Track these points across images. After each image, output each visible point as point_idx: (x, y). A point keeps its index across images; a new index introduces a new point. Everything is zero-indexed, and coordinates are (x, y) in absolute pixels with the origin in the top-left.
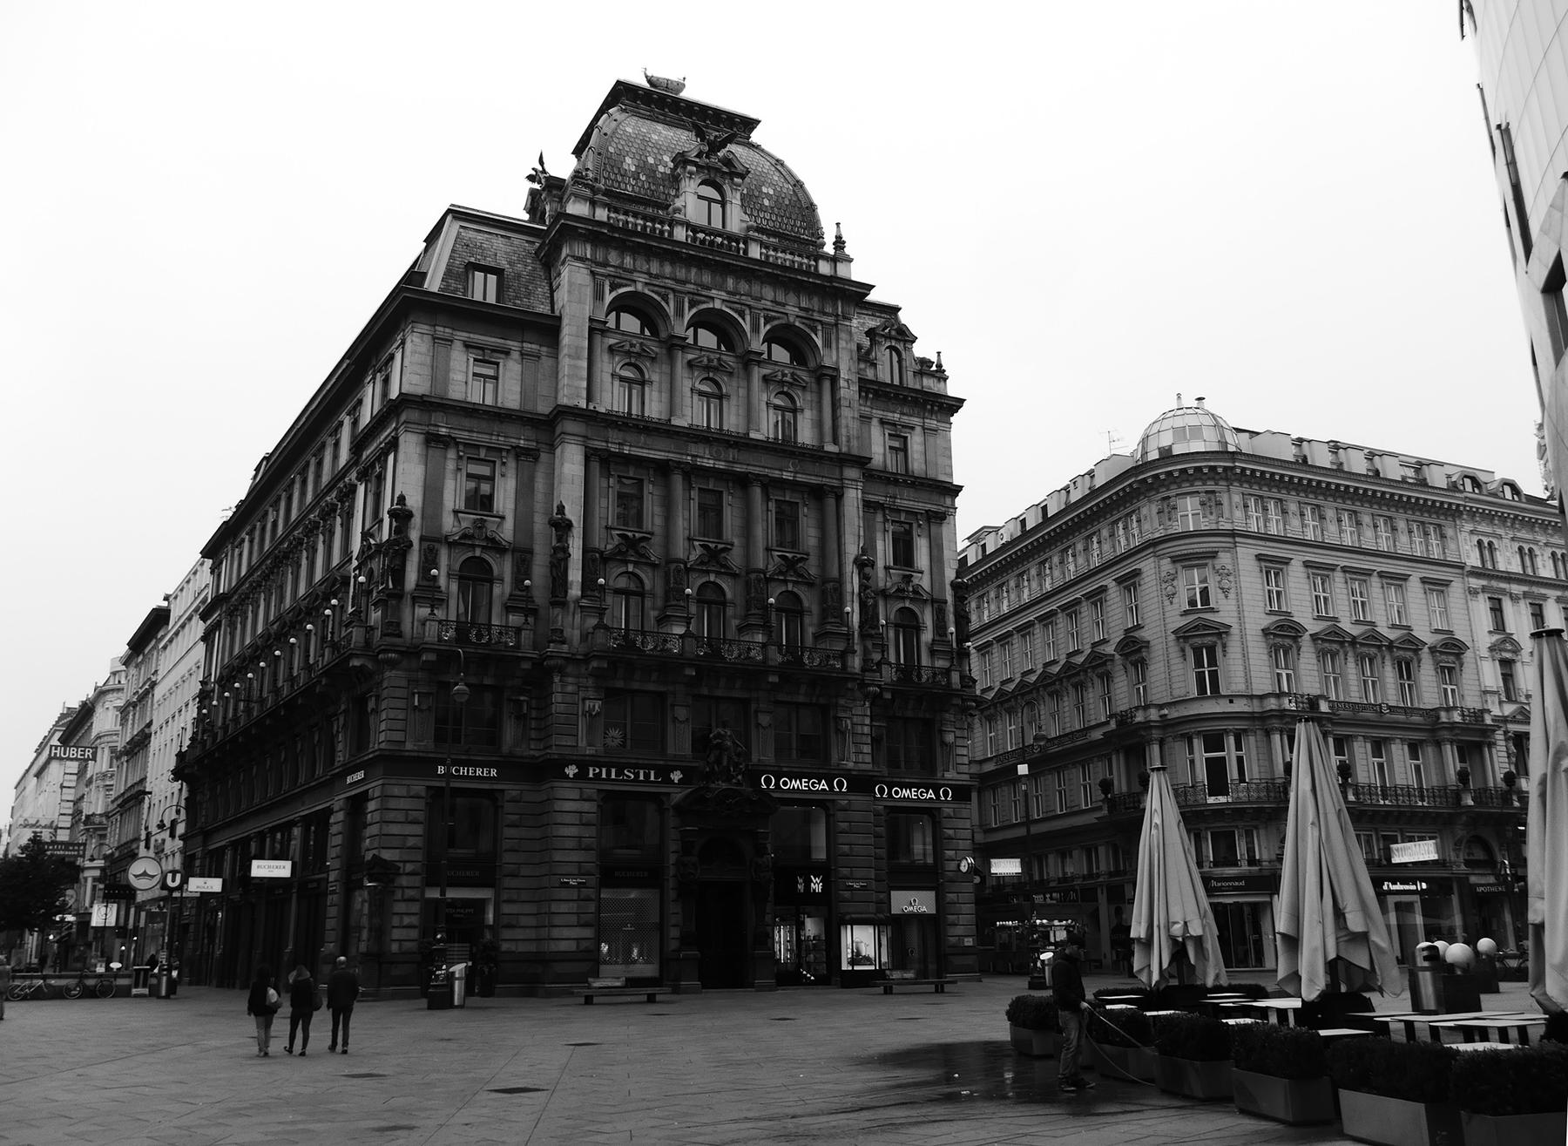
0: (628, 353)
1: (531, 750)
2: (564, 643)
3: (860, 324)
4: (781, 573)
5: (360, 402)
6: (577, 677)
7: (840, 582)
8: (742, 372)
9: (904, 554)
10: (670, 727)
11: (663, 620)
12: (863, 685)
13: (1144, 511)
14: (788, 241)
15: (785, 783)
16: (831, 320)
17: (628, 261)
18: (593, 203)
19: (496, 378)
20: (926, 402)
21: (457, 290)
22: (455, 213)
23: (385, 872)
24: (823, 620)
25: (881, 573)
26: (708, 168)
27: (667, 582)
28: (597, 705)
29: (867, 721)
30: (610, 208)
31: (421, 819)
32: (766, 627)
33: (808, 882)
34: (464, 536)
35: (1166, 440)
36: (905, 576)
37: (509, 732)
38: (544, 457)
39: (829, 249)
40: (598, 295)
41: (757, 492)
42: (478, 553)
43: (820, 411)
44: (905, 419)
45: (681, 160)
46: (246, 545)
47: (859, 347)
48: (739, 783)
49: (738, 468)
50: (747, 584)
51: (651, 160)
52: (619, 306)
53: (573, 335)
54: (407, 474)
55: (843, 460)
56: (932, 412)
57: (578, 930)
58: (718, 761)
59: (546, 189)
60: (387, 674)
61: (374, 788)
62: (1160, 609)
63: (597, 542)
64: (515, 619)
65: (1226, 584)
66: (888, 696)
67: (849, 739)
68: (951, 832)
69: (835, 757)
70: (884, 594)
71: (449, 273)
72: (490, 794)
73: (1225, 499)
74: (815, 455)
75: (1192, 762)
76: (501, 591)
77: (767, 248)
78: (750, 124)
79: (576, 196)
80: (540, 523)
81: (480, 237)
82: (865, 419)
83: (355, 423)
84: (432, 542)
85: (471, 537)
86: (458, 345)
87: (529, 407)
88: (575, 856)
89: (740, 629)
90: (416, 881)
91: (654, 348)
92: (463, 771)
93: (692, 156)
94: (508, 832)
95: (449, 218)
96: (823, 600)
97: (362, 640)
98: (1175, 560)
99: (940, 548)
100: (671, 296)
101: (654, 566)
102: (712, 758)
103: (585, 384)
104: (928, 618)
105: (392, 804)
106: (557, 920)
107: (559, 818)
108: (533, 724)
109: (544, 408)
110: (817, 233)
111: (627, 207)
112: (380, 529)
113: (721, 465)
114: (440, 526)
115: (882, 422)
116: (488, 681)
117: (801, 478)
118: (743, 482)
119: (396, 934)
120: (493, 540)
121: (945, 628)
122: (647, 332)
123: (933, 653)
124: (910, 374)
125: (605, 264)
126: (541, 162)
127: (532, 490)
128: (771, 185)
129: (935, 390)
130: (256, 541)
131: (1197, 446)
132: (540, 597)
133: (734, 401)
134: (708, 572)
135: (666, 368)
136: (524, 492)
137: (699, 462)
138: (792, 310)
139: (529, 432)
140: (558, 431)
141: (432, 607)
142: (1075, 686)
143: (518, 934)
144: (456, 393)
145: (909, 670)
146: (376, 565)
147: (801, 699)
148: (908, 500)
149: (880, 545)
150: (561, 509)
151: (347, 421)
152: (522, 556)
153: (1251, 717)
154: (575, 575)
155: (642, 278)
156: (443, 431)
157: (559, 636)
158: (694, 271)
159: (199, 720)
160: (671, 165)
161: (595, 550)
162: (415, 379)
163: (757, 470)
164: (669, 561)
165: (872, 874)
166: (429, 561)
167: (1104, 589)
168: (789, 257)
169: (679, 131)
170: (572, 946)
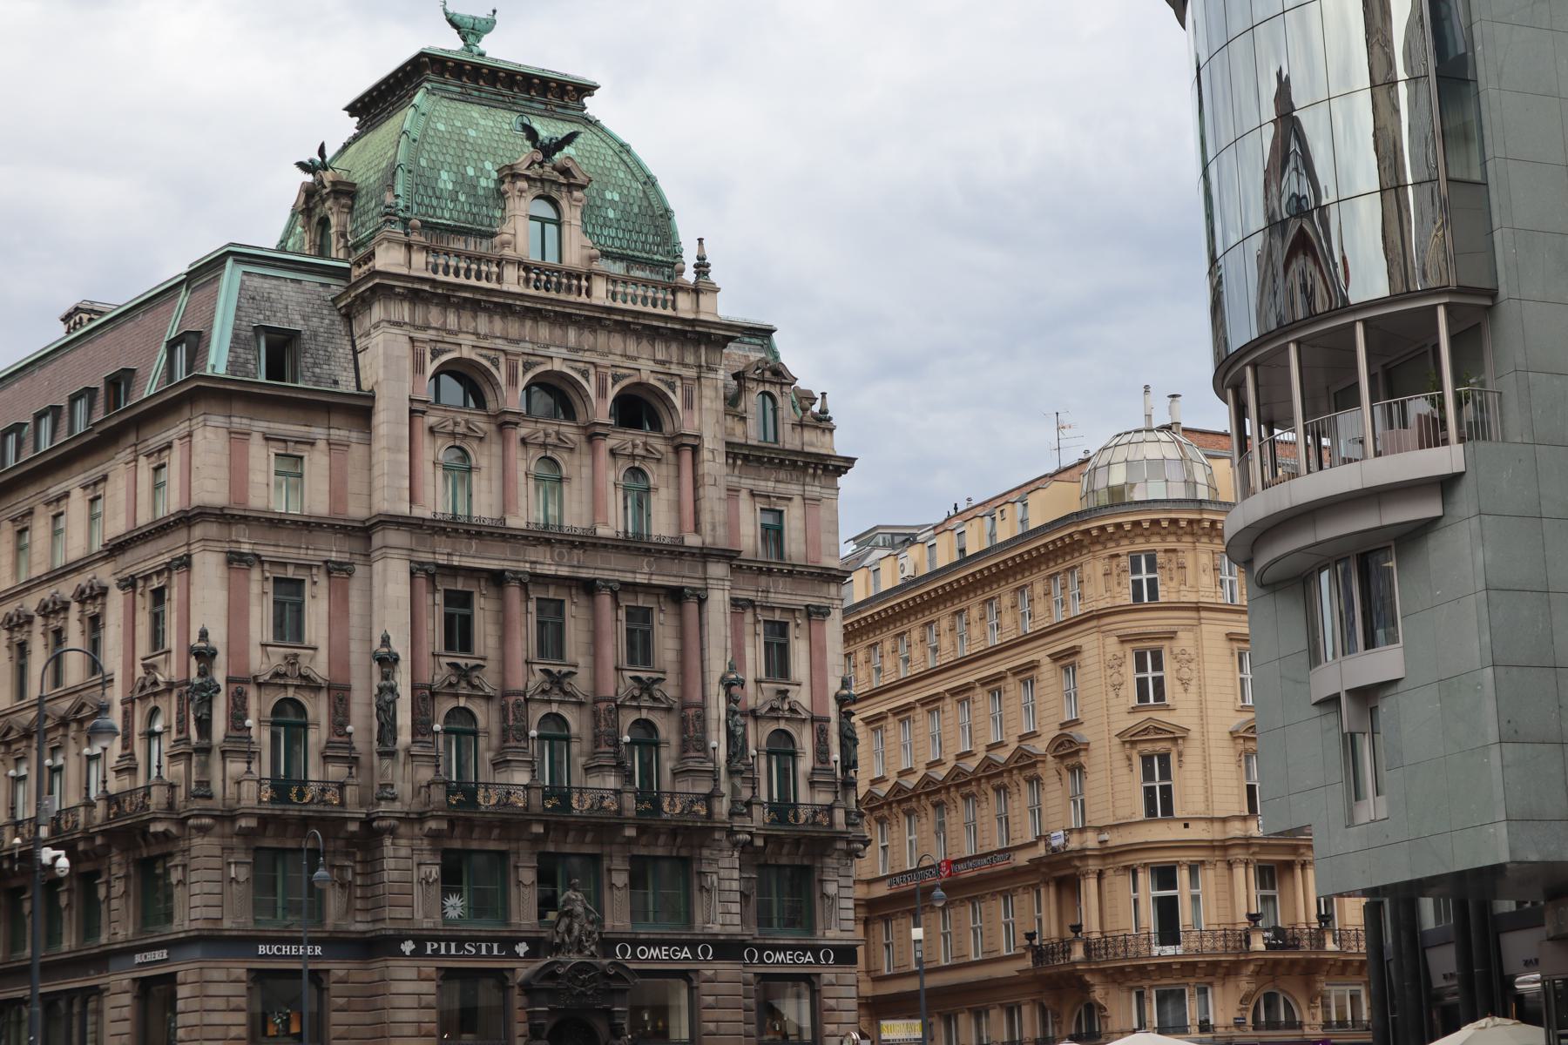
0: (453, 435)
1: (359, 925)
2: (394, 799)
4: (634, 698)
7: (702, 706)
8: (585, 447)
10: (514, 891)
11: (497, 765)
12: (731, 832)
13: (1087, 569)
15: (643, 952)
16: (692, 373)
17: (452, 320)
18: (409, 246)
20: (807, 465)
26: (542, 181)
27: (505, 718)
28: (435, 872)
29: (736, 874)
30: (426, 249)
32: (621, 768)
34: (277, 675)
35: (1118, 477)
37: (334, 903)
38: (359, 570)
39: (689, 276)
40: (419, 367)
41: (605, 600)
42: (290, 693)
43: (679, 488)
44: (782, 488)
45: (509, 174)
48: (592, 955)
49: (584, 574)
50: (595, 714)
51: (470, 171)
53: (389, 419)
54: (207, 599)
55: (705, 555)
56: (814, 475)
58: (569, 930)
60: (197, 841)
61: (186, 970)
62: (1103, 701)
63: (426, 678)
64: (336, 771)
65: (1185, 673)
66: (759, 842)
67: (715, 897)
68: (832, 1002)
70: (754, 714)
71: (236, 339)
72: (317, 977)
73: (1188, 559)
74: (674, 552)
75: (1136, 901)
77: (615, 282)
78: (586, 89)
79: (389, 241)
81: (267, 284)
82: (733, 492)
84: (240, 683)
89: (587, 770)
92: (286, 950)
95: (230, 262)
97: (164, 801)
98: (1124, 640)
99: (823, 651)
100: (502, 359)
101: (488, 698)
103: (406, 483)
107: (397, 1001)
108: (359, 893)
109: (356, 511)
113: (564, 571)
115: (752, 494)
117: (656, 580)
118: (589, 588)
120: (307, 678)
123: (812, 784)
124: (788, 427)
125: (427, 327)
128: (618, 186)
131: (1156, 491)
133: (575, 483)
134: (550, 702)
135: (496, 449)
137: (540, 569)
140: (377, 539)
142: (997, 789)
145: (783, 808)
147: (660, 852)
148: (783, 594)
150: (386, 641)
152: (339, 694)
153: (1211, 846)
154: (404, 718)
155: (467, 340)
156: (246, 548)
158: (528, 323)
160: (495, 175)
161: (423, 687)
162: (210, 485)
163: (607, 575)
164: (505, 694)
167: (1033, 666)
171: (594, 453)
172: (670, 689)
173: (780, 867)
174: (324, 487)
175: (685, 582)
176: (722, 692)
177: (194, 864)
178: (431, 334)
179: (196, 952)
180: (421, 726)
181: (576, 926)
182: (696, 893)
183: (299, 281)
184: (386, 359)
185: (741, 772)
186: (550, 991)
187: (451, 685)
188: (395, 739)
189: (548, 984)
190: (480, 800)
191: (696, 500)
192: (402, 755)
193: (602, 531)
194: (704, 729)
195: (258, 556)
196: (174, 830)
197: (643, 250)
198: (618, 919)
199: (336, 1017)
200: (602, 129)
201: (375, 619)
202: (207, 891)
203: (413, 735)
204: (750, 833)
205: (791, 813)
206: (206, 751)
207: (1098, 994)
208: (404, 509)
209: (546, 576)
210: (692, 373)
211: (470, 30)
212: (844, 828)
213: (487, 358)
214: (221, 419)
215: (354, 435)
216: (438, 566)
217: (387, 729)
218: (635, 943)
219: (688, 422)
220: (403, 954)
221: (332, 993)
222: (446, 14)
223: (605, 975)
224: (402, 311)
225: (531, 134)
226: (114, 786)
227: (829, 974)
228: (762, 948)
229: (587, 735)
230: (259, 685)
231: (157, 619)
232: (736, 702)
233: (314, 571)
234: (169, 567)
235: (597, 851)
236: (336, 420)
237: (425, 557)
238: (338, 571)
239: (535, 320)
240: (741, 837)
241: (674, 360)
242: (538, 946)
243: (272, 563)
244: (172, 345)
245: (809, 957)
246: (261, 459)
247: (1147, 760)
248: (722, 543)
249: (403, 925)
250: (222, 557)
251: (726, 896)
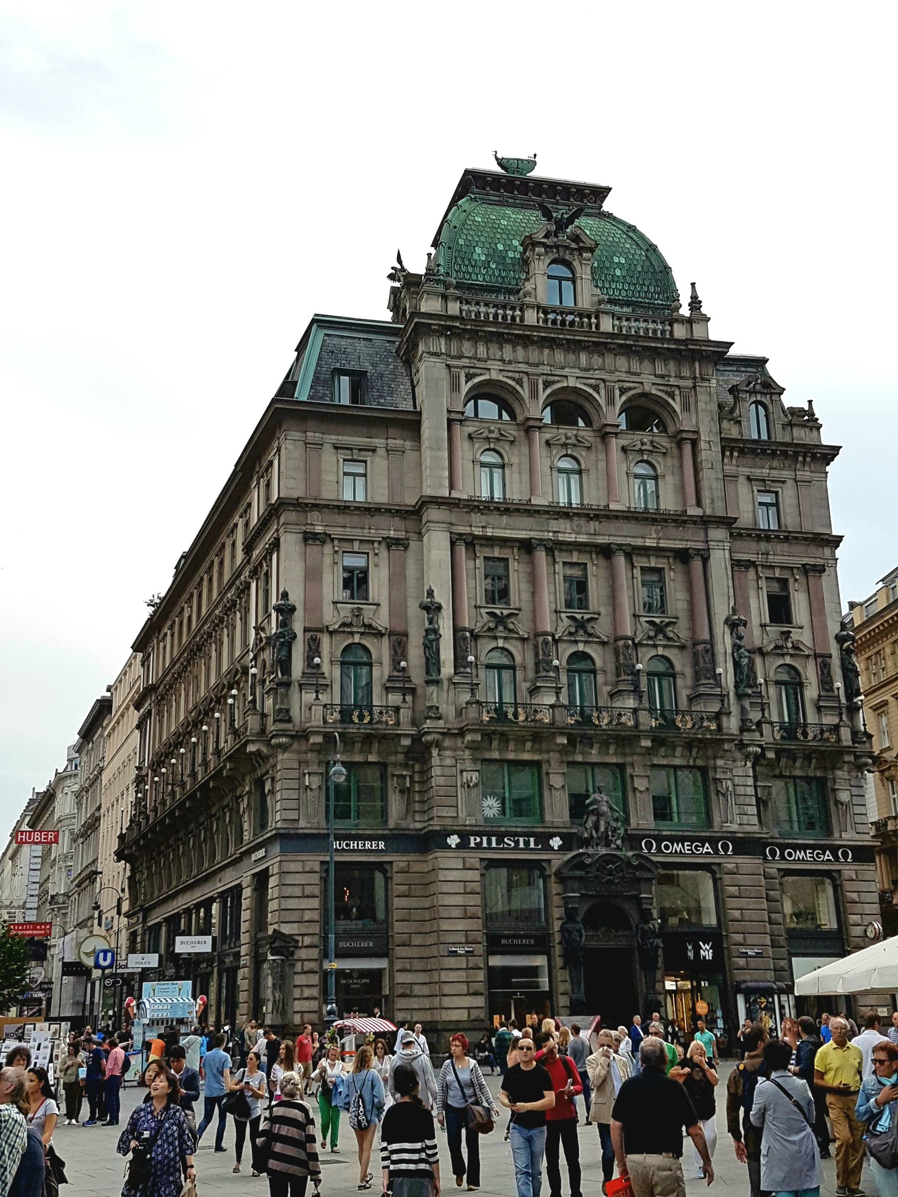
1: (416, 824)
2: (440, 718)
3: (717, 384)
4: (650, 638)
5: (249, 505)
6: (455, 750)
7: (711, 642)
8: (600, 447)
9: (780, 609)
12: (742, 746)
14: (638, 307)
15: (667, 847)
17: (482, 350)
18: (445, 298)
19: (365, 475)
20: (796, 454)
21: (325, 395)
22: (319, 322)
23: (285, 946)
24: (696, 686)
25: (757, 631)
26: (557, 247)
27: (536, 655)
29: (750, 781)
30: (460, 299)
31: (317, 893)
32: (636, 691)
33: (697, 949)
34: (344, 625)
36: (783, 633)
37: (396, 805)
39: (685, 311)
40: (455, 387)
41: (621, 561)
42: (357, 639)
43: (682, 474)
45: (529, 243)
46: (169, 638)
47: (720, 407)
48: (618, 848)
49: (600, 540)
51: (500, 247)
52: (476, 395)
53: (433, 427)
54: (289, 571)
55: (705, 522)
57: (469, 998)
58: (596, 827)
59: (405, 286)
64: (395, 699)
66: (771, 755)
67: (731, 800)
68: (854, 896)
69: (717, 820)
70: (760, 651)
71: (316, 380)
72: (381, 867)
74: (680, 520)
76: (381, 673)
77: (619, 319)
78: (601, 193)
80: (413, 608)
81: (343, 342)
83: (247, 525)
84: (314, 633)
85: (350, 625)
86: (328, 448)
87: (397, 500)
88: (461, 925)
90: (314, 953)
91: (512, 432)
92: (353, 845)
93: (540, 237)
95: (314, 327)
96: (696, 663)
100: (525, 380)
102: (590, 824)
103: (446, 474)
104: (810, 673)
105: (289, 879)
106: (447, 989)
107: (446, 888)
108: (417, 798)
109: (411, 500)
110: (674, 297)
111: (480, 297)
112: (269, 622)
113: (582, 538)
114: (321, 618)
115: (749, 479)
116: (372, 758)
117: (663, 544)
118: (606, 552)
120: (370, 626)
121: (831, 683)
122: (506, 417)
123: (819, 709)
124: (779, 427)
125: (461, 357)
126: (399, 260)
127: (404, 577)
128: (625, 254)
129: (807, 441)
130: (176, 635)
132: (417, 676)
133: (593, 472)
134: (576, 642)
135: (525, 450)
136: (397, 579)
137: (561, 537)
139: (397, 522)
141: (317, 692)
143: (414, 1003)
144: (328, 494)
146: (267, 655)
147: (678, 762)
148: (782, 555)
149: (753, 602)
150: (430, 593)
151: (241, 523)
154: (447, 654)
155: (495, 366)
156: (319, 529)
157: (434, 713)
158: (546, 351)
159: (138, 803)
160: (521, 249)
163: (620, 540)
164: (536, 635)
165: (768, 940)
166: (313, 649)
168: (643, 325)
170: (463, 1015)
172: (682, 631)
173: (795, 778)
175: (689, 545)
176: (727, 631)
177: (278, 776)
178: (465, 362)
179: (276, 849)
180: (459, 661)
181: (602, 823)
182: (713, 796)
183: (370, 340)
184: (433, 388)
185: (749, 696)
186: (580, 879)
187: (490, 629)
188: (439, 671)
189: (577, 873)
190: (510, 716)
192: (445, 684)
193: (612, 507)
195: (330, 535)
196: (265, 750)
197: (646, 297)
198: (642, 818)
199: (397, 902)
200: (615, 219)
202: (292, 797)
203: (455, 669)
204: (760, 746)
205: (799, 731)
206: (288, 685)
209: (569, 544)
210: (690, 383)
212: (850, 744)
213: (513, 379)
214: (298, 434)
215: (408, 444)
216: (476, 537)
217: (432, 661)
218: (659, 839)
219: (686, 423)
220: (450, 847)
221: (395, 881)
222: (497, 159)
223: (629, 864)
224: (441, 345)
227: (849, 870)
228: (783, 847)
229: (611, 667)
230: (331, 633)
231: (267, 592)
232: (740, 638)
233: (376, 545)
235: (621, 761)
236: (392, 431)
239: (551, 348)
240: (751, 749)
241: (673, 374)
242: (569, 841)
243: (340, 540)
245: (828, 856)
248: (720, 513)
249: (448, 822)
250: (300, 536)
251: (741, 800)
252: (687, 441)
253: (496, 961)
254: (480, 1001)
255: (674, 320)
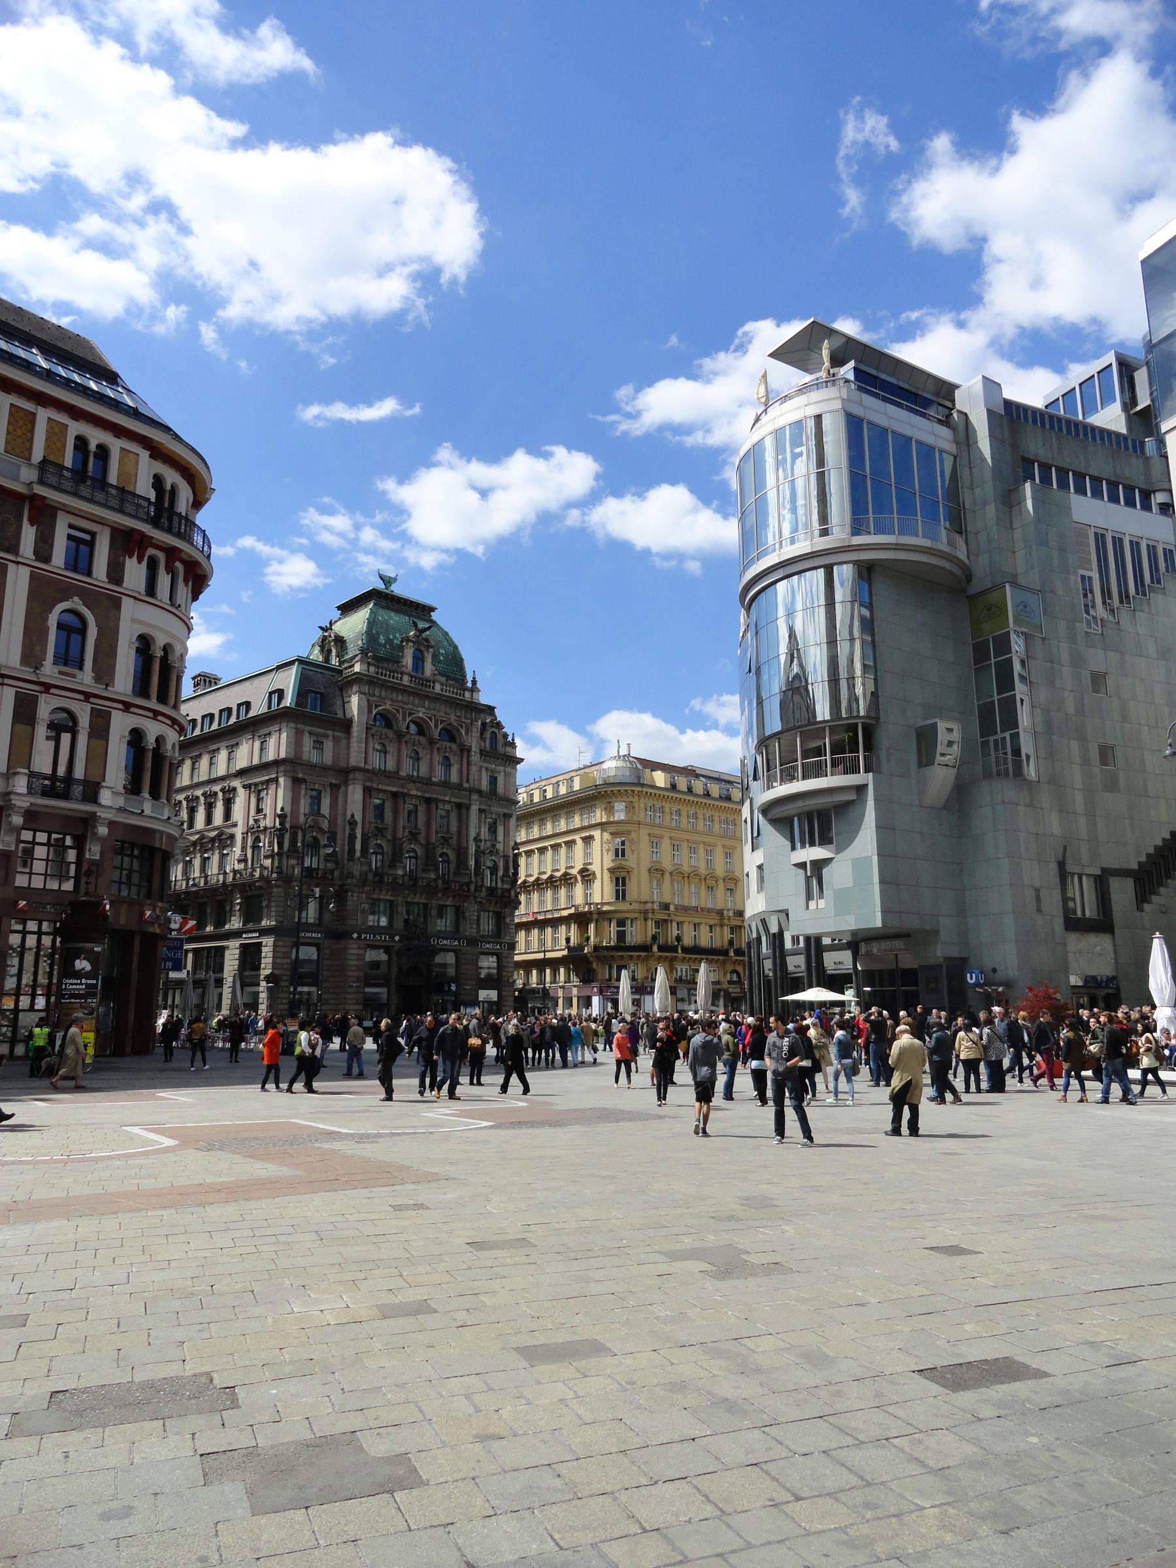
7: (467, 848)
16: (468, 721)
17: (383, 693)
18: (369, 664)
33: (450, 986)
38: (343, 788)
39: (469, 685)
40: (370, 711)
49: (427, 795)
53: (357, 731)
55: (472, 791)
60: (275, 890)
64: (330, 866)
70: (483, 852)
73: (636, 805)
78: (433, 609)
82: (481, 768)
84: (295, 828)
88: (355, 974)
89: (423, 871)
92: (308, 935)
94: (325, 962)
104: (501, 865)
105: (279, 949)
109: (342, 764)
113: (419, 794)
118: (428, 801)
119: (280, 1007)
123: (503, 881)
125: (374, 695)
128: (444, 648)
138: (453, 717)
140: (351, 776)
150: (353, 816)
152: (333, 837)
154: (358, 846)
156: (300, 776)
157: (350, 875)
167: (573, 842)
169: (402, 616)
171: (432, 751)
174: (331, 755)
180: (364, 850)
191: (468, 770)
194: (467, 858)
201: (348, 807)
207: (594, 965)
208: (362, 765)
211: (387, 581)
225: (415, 625)
226: (238, 867)
234: (268, 782)
237: (368, 784)
238: (334, 788)
244: (271, 694)
246: (308, 742)
247: (617, 879)
252: (465, 750)
253: (367, 990)
254: (360, 1007)
255: (466, 689)
